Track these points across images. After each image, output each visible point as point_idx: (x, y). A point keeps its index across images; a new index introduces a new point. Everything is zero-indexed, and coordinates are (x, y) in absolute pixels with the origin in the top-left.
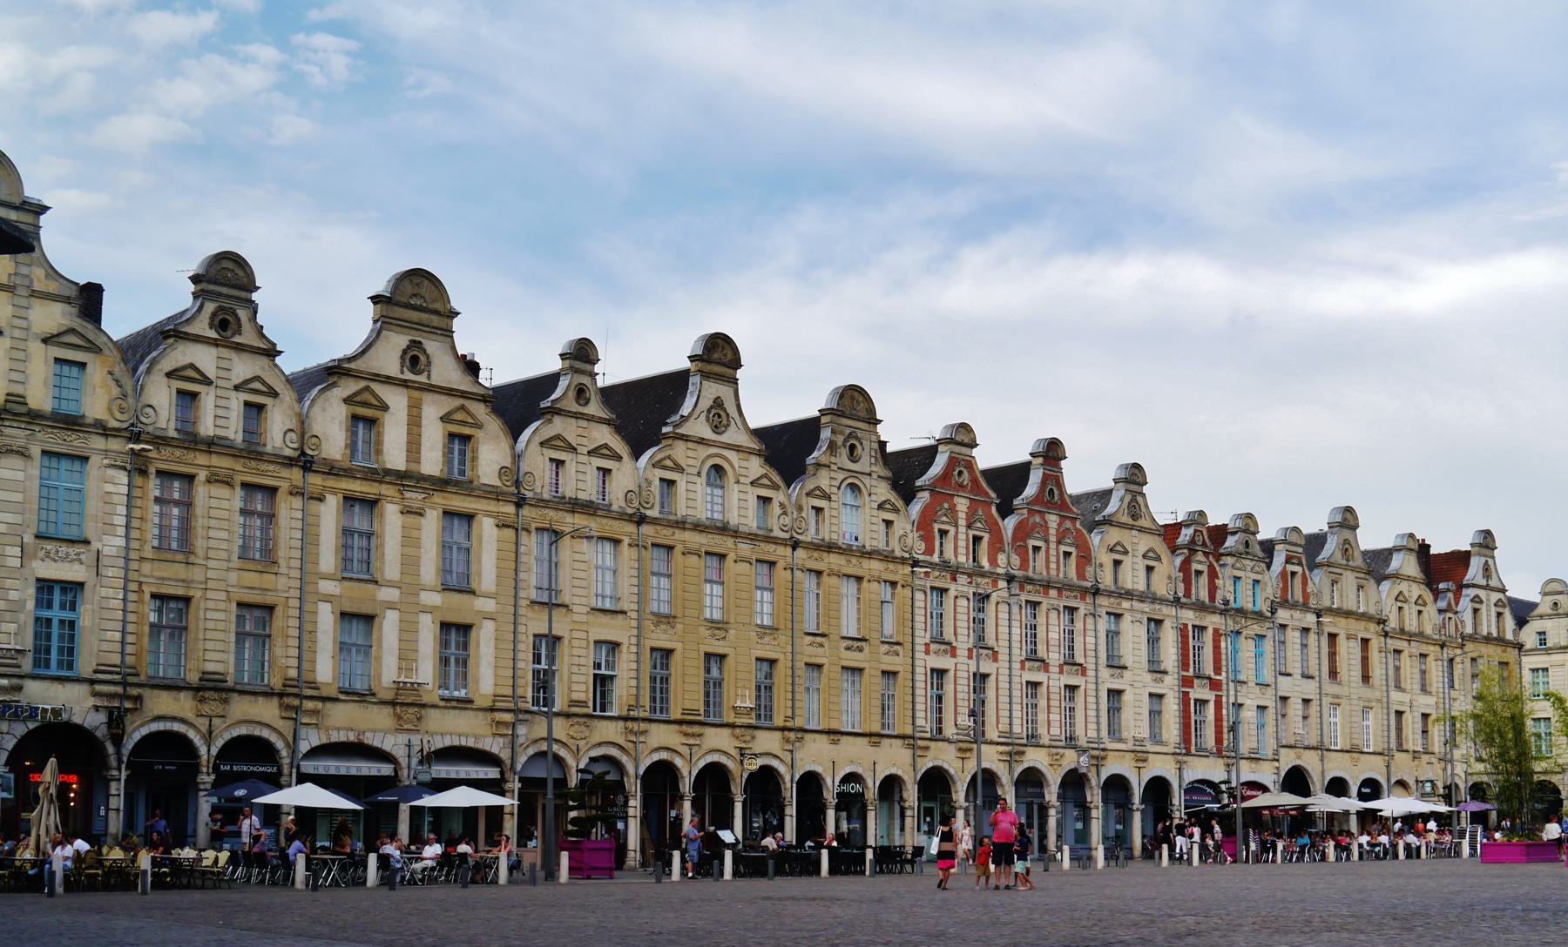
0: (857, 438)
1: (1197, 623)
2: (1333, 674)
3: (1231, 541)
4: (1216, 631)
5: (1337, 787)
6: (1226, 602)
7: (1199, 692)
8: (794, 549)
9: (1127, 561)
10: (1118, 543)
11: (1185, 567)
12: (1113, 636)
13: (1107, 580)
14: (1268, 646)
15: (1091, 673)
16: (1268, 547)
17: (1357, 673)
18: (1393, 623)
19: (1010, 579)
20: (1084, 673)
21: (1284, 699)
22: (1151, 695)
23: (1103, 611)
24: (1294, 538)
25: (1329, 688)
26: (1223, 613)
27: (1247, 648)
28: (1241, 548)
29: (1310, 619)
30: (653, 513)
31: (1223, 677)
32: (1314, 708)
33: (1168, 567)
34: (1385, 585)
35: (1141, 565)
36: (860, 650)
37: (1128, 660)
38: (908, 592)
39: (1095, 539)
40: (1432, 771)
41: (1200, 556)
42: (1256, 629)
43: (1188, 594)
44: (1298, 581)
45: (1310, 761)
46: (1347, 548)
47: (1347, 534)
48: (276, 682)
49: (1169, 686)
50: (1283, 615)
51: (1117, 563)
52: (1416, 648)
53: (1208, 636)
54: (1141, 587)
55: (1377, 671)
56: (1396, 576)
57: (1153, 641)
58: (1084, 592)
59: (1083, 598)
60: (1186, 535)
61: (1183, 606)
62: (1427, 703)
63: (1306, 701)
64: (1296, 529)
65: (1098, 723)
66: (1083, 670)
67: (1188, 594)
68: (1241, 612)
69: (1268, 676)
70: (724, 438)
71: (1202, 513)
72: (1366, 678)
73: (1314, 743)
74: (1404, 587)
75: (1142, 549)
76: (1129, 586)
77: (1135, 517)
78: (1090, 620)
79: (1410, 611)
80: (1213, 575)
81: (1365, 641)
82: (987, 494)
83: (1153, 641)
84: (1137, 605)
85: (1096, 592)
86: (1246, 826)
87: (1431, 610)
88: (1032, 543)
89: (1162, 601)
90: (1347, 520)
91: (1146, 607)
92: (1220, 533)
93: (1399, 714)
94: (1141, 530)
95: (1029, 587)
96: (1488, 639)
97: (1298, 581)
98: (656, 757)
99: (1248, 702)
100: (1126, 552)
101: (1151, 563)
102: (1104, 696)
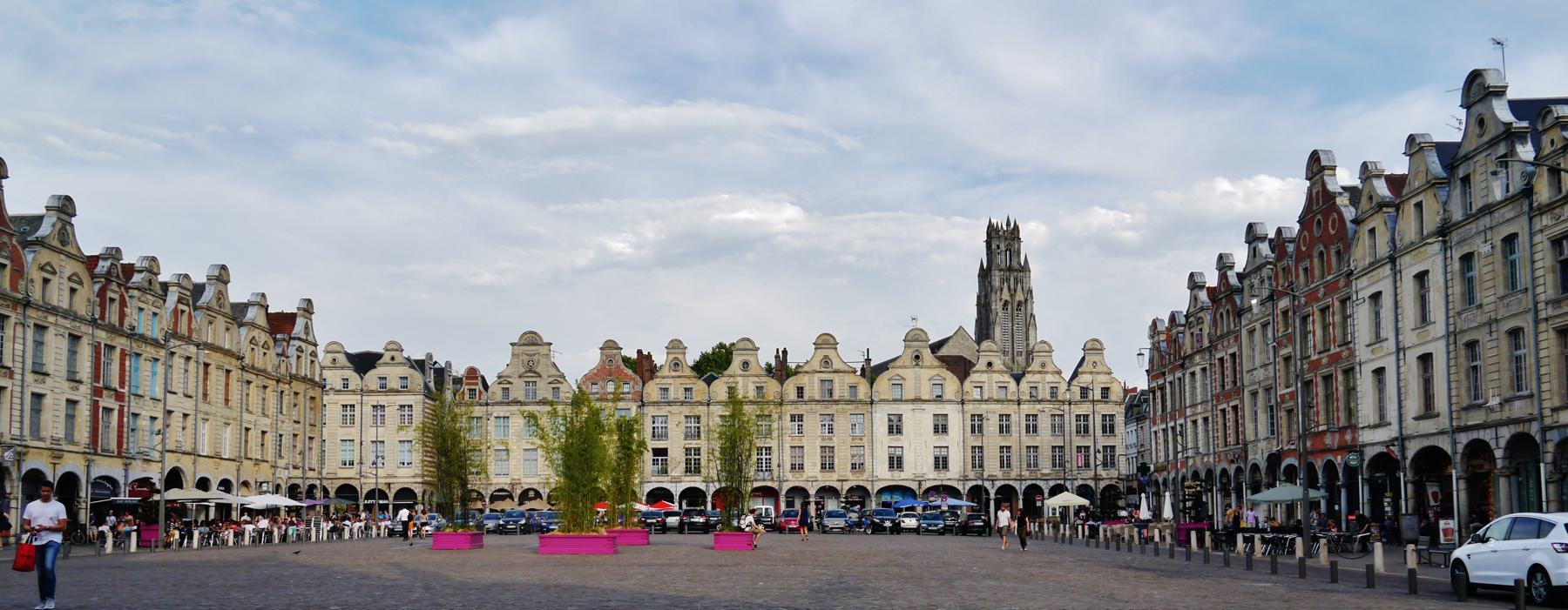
2: (205, 395)
3: (137, 278)
4: (123, 351)
5: (203, 484)
7: (107, 401)
9: (55, 280)
10: (48, 264)
11: (102, 293)
12: (39, 344)
13: (36, 295)
14: (160, 368)
15: (18, 377)
16: (165, 286)
17: (222, 397)
18: (247, 361)
20: (11, 374)
21: (170, 412)
22: (68, 401)
23: (31, 322)
24: (184, 283)
25: (203, 407)
26: (129, 336)
27: (146, 366)
28: (146, 285)
29: (193, 349)
31: (126, 390)
32: (190, 420)
33: (88, 291)
34: (244, 330)
35: (67, 285)
37: (50, 368)
39: (29, 258)
40: (283, 476)
41: (114, 287)
42: (150, 351)
44: (185, 316)
45: (185, 464)
46: (221, 296)
47: (221, 286)
49: (83, 394)
50: (173, 342)
51: (46, 281)
52: (260, 381)
53: (117, 354)
54: (65, 305)
55: (235, 397)
56: (253, 325)
57: (73, 353)
58: (16, 303)
59: (15, 309)
60: (103, 266)
62: (265, 423)
63: (185, 416)
64: (186, 276)
66: (11, 374)
67: (102, 317)
68: (143, 338)
69: (159, 394)
71: (118, 250)
72: (227, 401)
73: (189, 449)
74: (256, 333)
75: (68, 273)
76: (55, 303)
77: (64, 243)
78: (19, 329)
79: (259, 351)
80: (123, 304)
81: (228, 372)
83: (73, 353)
84: (61, 321)
85: (27, 304)
86: (168, 518)
87: (272, 353)
89: (82, 320)
90: (222, 276)
91: (67, 323)
92: (129, 270)
93: (247, 429)
94: (69, 255)
96: (304, 379)
97: (185, 316)
99: (144, 413)
100: (54, 273)
101: (75, 286)
102: (28, 398)
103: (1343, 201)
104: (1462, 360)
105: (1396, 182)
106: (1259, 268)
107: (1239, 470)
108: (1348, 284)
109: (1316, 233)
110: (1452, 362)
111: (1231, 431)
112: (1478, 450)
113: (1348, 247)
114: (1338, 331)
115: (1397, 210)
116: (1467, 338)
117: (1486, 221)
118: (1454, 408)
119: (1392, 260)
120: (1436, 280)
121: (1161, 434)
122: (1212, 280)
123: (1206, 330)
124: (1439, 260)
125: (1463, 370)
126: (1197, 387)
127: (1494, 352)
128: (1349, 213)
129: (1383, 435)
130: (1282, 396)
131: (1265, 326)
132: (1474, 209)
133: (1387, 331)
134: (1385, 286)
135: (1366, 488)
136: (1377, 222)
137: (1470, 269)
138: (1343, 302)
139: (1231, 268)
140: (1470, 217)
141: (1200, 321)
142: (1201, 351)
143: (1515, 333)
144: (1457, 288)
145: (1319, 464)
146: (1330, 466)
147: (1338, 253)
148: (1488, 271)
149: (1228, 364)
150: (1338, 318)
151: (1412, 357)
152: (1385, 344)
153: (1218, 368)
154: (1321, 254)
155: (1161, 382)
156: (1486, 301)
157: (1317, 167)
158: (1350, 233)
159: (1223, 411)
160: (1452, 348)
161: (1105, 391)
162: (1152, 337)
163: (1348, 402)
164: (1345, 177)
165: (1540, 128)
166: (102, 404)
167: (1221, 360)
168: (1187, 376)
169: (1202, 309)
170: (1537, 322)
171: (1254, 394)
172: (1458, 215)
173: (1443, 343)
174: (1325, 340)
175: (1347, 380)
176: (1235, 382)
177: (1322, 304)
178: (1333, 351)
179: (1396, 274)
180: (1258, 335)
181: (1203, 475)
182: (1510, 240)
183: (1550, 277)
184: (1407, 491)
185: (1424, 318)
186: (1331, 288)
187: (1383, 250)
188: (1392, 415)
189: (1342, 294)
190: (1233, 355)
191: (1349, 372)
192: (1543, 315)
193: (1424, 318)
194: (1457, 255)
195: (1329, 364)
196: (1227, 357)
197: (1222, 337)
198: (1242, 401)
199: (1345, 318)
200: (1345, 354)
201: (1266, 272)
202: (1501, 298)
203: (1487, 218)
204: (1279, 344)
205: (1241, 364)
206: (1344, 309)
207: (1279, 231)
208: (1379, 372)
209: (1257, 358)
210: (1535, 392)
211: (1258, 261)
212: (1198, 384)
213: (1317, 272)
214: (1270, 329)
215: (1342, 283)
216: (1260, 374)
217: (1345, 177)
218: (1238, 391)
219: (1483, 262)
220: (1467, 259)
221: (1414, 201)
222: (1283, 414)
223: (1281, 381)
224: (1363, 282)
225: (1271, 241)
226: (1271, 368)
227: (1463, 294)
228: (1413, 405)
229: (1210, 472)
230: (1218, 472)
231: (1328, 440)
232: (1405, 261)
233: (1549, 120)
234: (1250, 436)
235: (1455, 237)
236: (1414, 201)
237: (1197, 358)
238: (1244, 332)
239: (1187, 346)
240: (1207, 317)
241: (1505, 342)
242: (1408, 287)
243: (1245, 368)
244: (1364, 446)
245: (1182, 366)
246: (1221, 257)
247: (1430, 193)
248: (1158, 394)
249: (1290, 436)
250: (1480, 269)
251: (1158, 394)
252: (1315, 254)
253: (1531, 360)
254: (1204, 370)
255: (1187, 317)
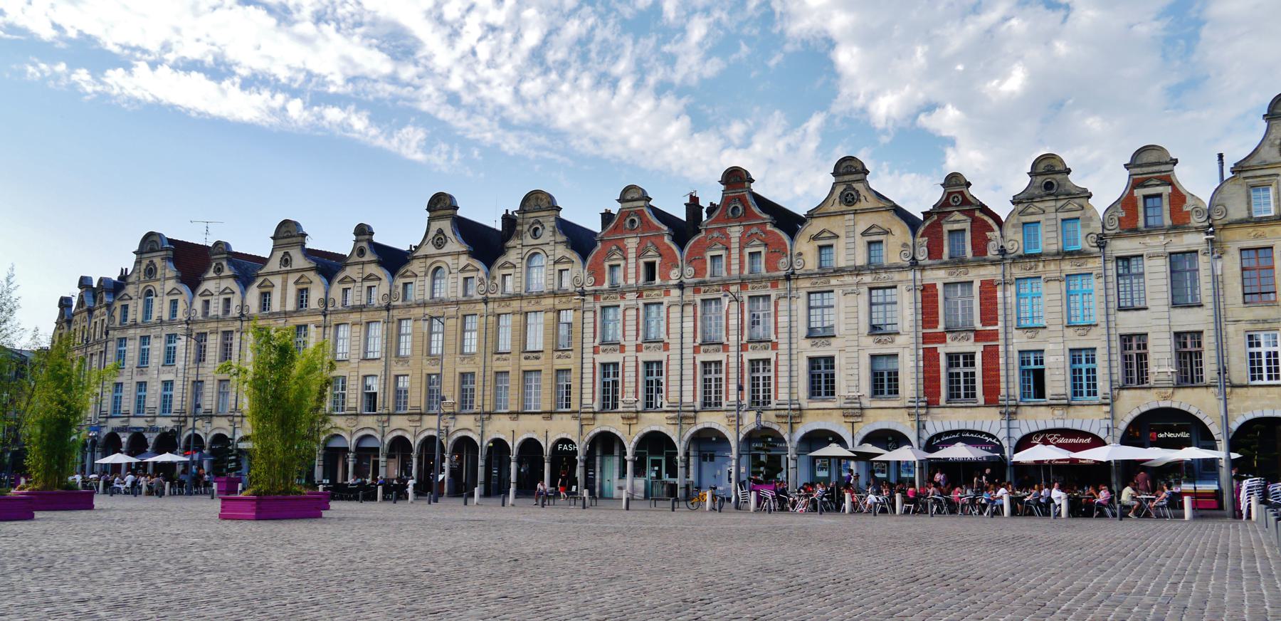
0: (539, 222)
1: (952, 279)
6: (1003, 251)
8: (486, 304)
10: (823, 231)
15: (783, 347)
19: (681, 286)
30: (399, 303)
35: (861, 243)
36: (537, 358)
38: (579, 313)
41: (957, 216)
43: (934, 252)
48: (227, 411)
58: (774, 282)
61: (923, 268)
65: (594, 392)
70: (444, 251)
82: (659, 229)
88: (709, 254)
94: (855, 212)
95: (703, 289)
98: (395, 434)
99: (1048, 347)
166: (942, 350)
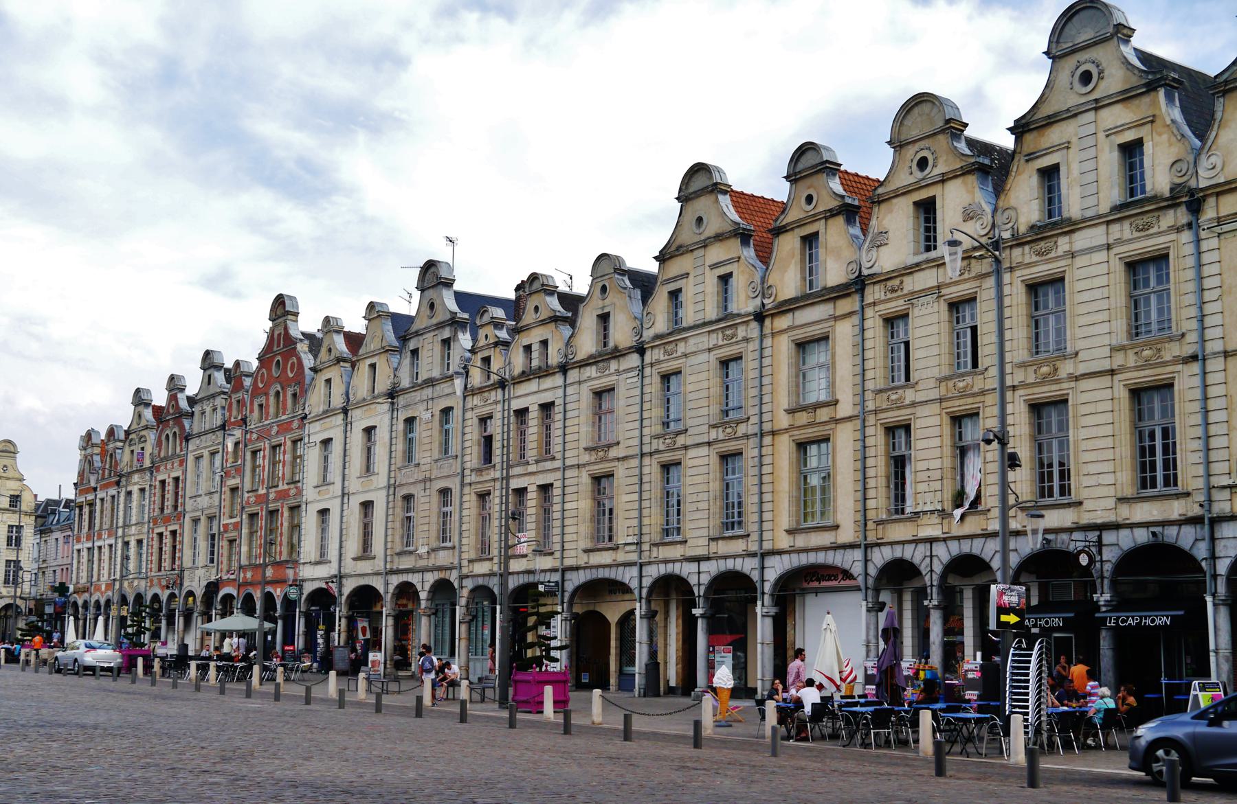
103: (302, 347)
104: (399, 510)
105: (354, 341)
106: (213, 396)
107: (172, 596)
108: (302, 427)
109: (275, 373)
110: (390, 512)
111: (167, 556)
112: (406, 591)
113: (304, 392)
114: (288, 469)
115: (353, 366)
116: (404, 491)
117: (428, 392)
118: (389, 552)
119: (345, 411)
120: (382, 435)
121: (85, 553)
122: (160, 398)
123: (148, 450)
124: (387, 417)
125: (398, 519)
126: (136, 506)
127: (426, 506)
128: (308, 361)
129: (323, 571)
130: (226, 526)
131: (213, 454)
132: (420, 381)
133: (335, 475)
134: (337, 434)
135: (302, 621)
136: (333, 373)
137: (411, 431)
138: (295, 442)
139: (182, 390)
140: (416, 386)
141: (142, 439)
142: (141, 470)
143: (445, 492)
144: (400, 446)
145: (258, 595)
146: (269, 599)
147: (294, 395)
148: (427, 433)
149: (170, 488)
150: (288, 457)
151: (355, 502)
152: (331, 487)
153: (158, 491)
154: (278, 393)
155: (90, 497)
156: (422, 461)
157: (282, 308)
158: (307, 381)
159: (161, 535)
160: (391, 498)
161: (15, 500)
162: (84, 448)
163: (291, 537)
164: (308, 322)
165: (478, 323)
167: (163, 482)
168: (122, 495)
169: (146, 428)
170: (462, 485)
171: (196, 521)
172: (405, 382)
173: (384, 492)
174: (273, 474)
175: (292, 517)
176: (176, 507)
177: (275, 441)
178: (281, 487)
179: (347, 423)
180: (205, 462)
181: (131, 599)
182: (446, 411)
183: (475, 448)
184: (341, 625)
185: (368, 469)
186: (285, 428)
187: (337, 401)
188: (333, 553)
189: (295, 435)
190: (177, 479)
191: (295, 509)
192: (467, 480)
193: (368, 469)
194: (402, 416)
195: (276, 500)
196: (170, 481)
197: (166, 459)
198: (182, 526)
199: (295, 458)
200: (293, 492)
201: (219, 401)
202: (436, 461)
203: (430, 389)
204: (226, 475)
205: (184, 489)
206: (294, 449)
207: (237, 364)
208: (324, 512)
209: (202, 485)
210: (457, 545)
211: (213, 389)
212: (134, 504)
213: (272, 410)
214: (218, 458)
215: (295, 424)
216: (204, 502)
217: (308, 322)
218: (179, 515)
219: (424, 427)
220: (410, 421)
221: (369, 361)
222: (225, 543)
223: (226, 510)
224: (316, 427)
225: (227, 370)
226: (216, 496)
227: (404, 452)
228: (353, 546)
229: (139, 597)
230: (149, 598)
231: (269, 572)
232: (355, 414)
233: (486, 318)
234: (187, 563)
235: (401, 401)
236: (369, 361)
237: (136, 478)
238: (191, 458)
239: (125, 458)
240: (151, 436)
241: (436, 499)
242: (357, 437)
243: (188, 494)
244: (303, 580)
245: (118, 483)
246: (172, 378)
247: (384, 357)
248: (86, 510)
249: (229, 565)
250: (419, 431)
251: (86, 510)
252: (272, 392)
253: (456, 517)
254: (142, 490)
255: (127, 433)
